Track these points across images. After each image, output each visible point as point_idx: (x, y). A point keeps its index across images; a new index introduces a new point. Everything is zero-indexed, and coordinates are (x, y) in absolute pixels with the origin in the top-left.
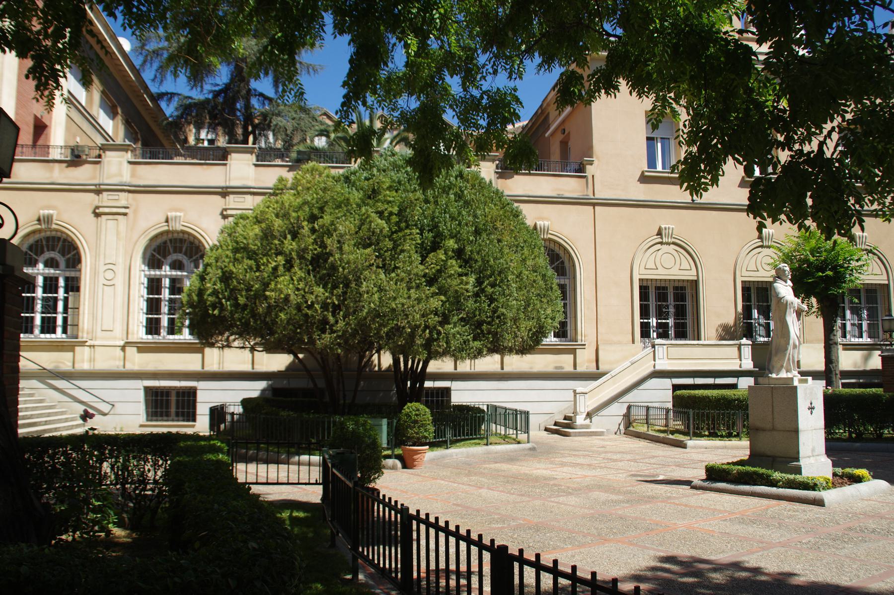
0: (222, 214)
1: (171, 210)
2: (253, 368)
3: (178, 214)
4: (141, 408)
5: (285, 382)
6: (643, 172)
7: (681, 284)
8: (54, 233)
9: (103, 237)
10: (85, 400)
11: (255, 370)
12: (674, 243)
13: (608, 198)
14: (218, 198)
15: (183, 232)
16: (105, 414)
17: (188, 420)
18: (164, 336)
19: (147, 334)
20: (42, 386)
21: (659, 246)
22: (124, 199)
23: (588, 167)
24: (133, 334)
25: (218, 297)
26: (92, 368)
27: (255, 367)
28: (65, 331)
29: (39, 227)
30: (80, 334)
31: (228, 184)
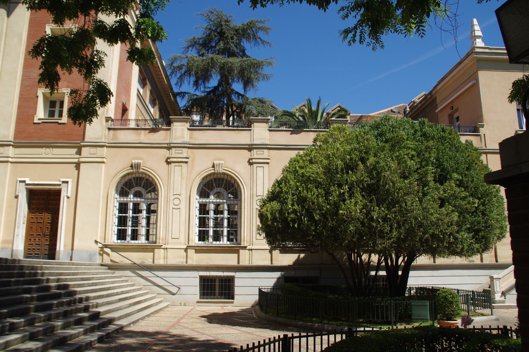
0: (249, 162)
1: (216, 160)
2: (272, 263)
3: (221, 162)
4: (197, 290)
5: (293, 273)
6: (516, 131)
8: (141, 175)
9: (172, 177)
10: (161, 285)
11: (273, 265)
14: (246, 151)
15: (224, 174)
16: (174, 294)
17: (229, 299)
18: (211, 242)
19: (200, 240)
20: (132, 274)
22: (185, 152)
23: (481, 129)
24: (192, 241)
25: (297, 215)
26: (165, 263)
27: (273, 262)
28: (147, 239)
29: (132, 171)
30: (158, 241)
31: (252, 143)
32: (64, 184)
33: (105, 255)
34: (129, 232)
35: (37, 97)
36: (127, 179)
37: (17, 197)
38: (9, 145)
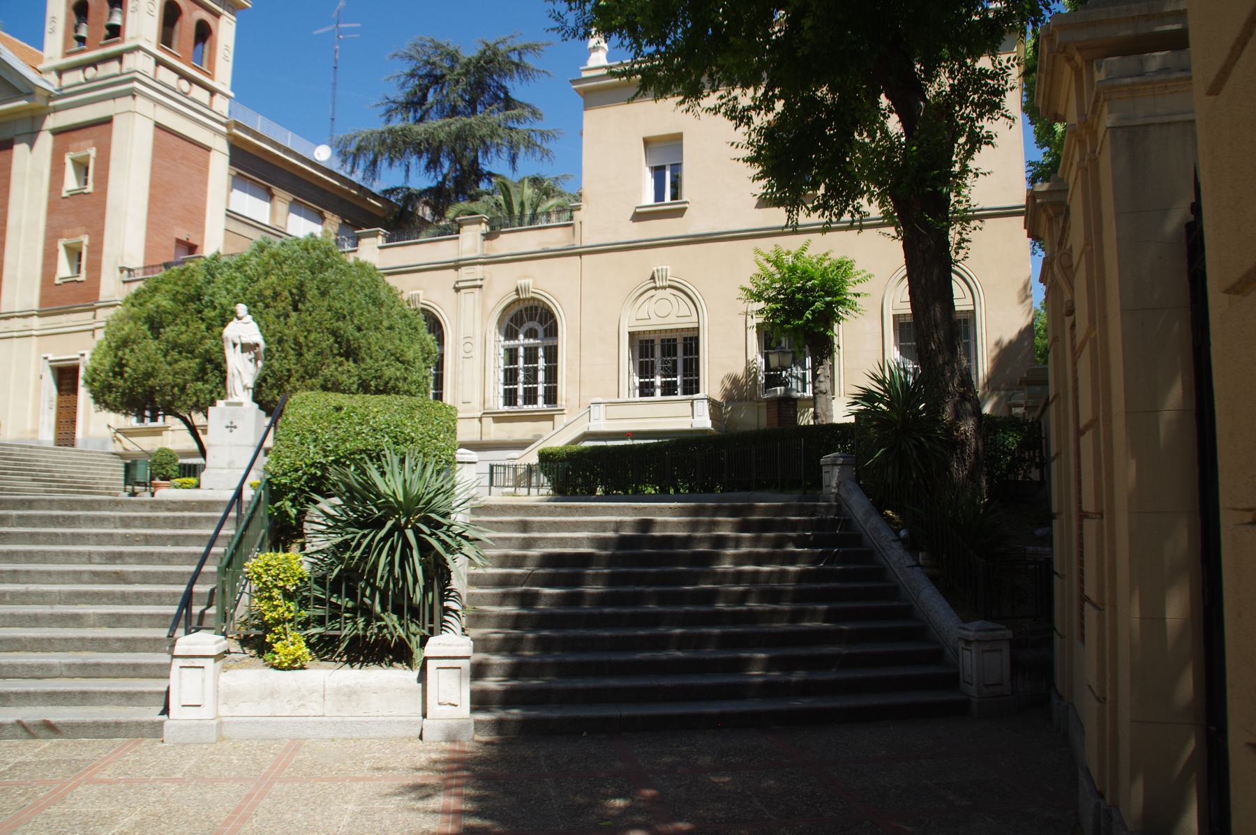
7: (668, 336)
12: (671, 287)
13: (594, 243)
21: (653, 292)
32: (82, 358)
33: (117, 442)
35: (58, 250)
37: (41, 377)
38: (32, 315)
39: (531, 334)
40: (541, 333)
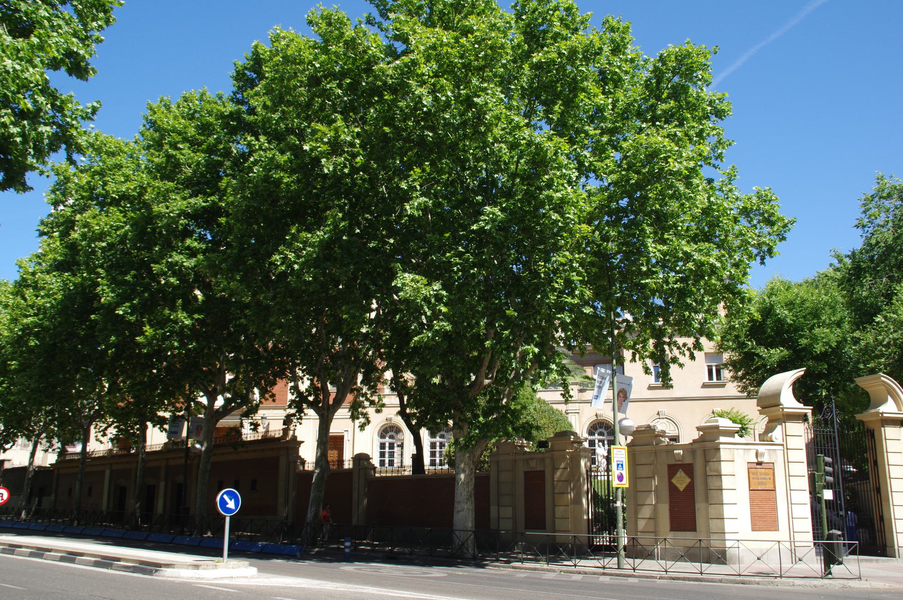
34: (387, 461)
36: (384, 427)
39: (601, 434)
40: (605, 433)
